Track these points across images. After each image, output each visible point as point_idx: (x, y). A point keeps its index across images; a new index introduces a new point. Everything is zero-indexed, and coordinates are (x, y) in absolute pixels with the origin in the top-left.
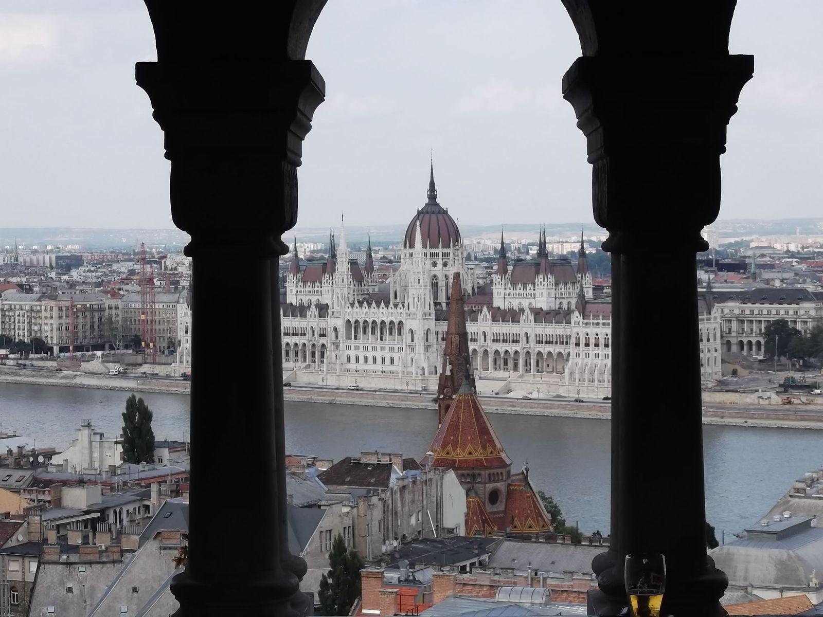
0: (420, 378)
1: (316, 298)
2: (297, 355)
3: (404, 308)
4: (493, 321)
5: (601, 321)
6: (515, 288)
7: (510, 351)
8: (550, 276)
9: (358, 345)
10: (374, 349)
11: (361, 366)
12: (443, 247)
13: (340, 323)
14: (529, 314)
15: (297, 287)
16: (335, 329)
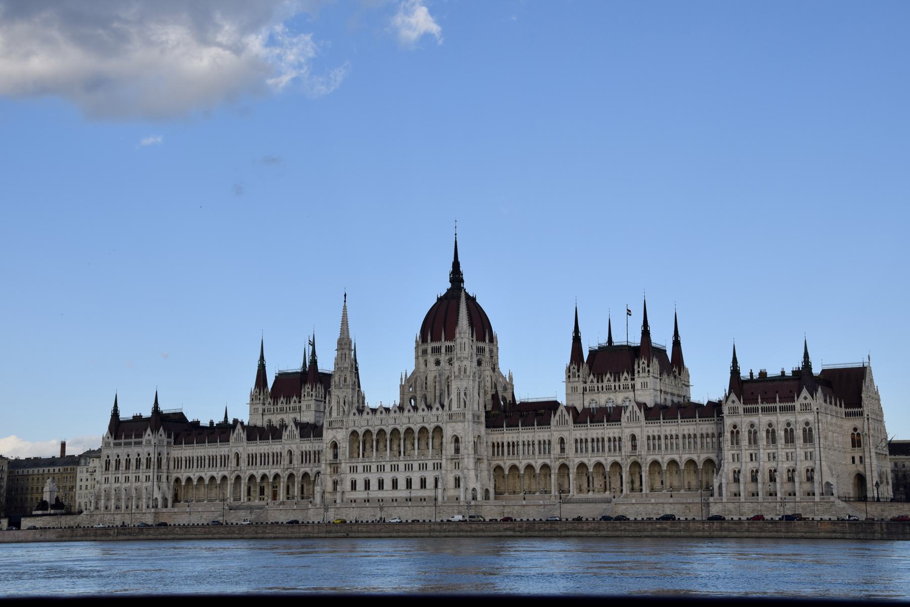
0: (473, 503)
1: (292, 416)
2: (262, 492)
3: (443, 406)
4: (575, 422)
5: (778, 405)
6: (600, 379)
7: (604, 462)
8: (655, 359)
9: (368, 464)
10: (395, 468)
11: (374, 493)
12: (477, 340)
13: (341, 436)
14: (636, 408)
15: (264, 404)
16: (335, 446)
